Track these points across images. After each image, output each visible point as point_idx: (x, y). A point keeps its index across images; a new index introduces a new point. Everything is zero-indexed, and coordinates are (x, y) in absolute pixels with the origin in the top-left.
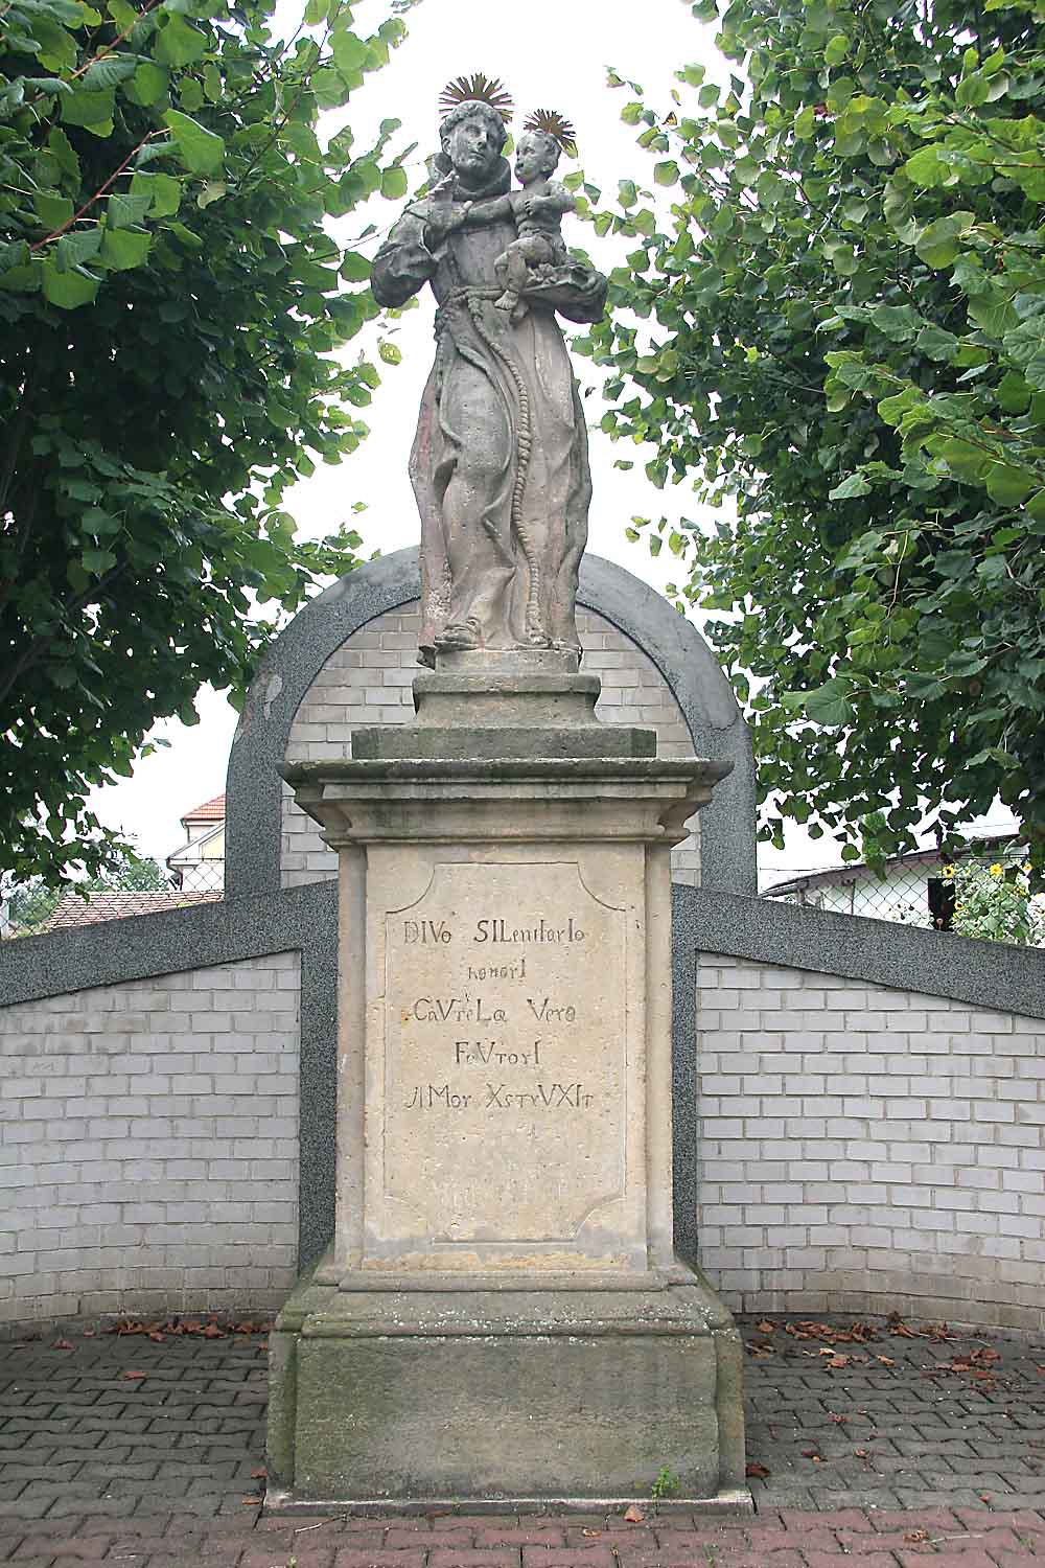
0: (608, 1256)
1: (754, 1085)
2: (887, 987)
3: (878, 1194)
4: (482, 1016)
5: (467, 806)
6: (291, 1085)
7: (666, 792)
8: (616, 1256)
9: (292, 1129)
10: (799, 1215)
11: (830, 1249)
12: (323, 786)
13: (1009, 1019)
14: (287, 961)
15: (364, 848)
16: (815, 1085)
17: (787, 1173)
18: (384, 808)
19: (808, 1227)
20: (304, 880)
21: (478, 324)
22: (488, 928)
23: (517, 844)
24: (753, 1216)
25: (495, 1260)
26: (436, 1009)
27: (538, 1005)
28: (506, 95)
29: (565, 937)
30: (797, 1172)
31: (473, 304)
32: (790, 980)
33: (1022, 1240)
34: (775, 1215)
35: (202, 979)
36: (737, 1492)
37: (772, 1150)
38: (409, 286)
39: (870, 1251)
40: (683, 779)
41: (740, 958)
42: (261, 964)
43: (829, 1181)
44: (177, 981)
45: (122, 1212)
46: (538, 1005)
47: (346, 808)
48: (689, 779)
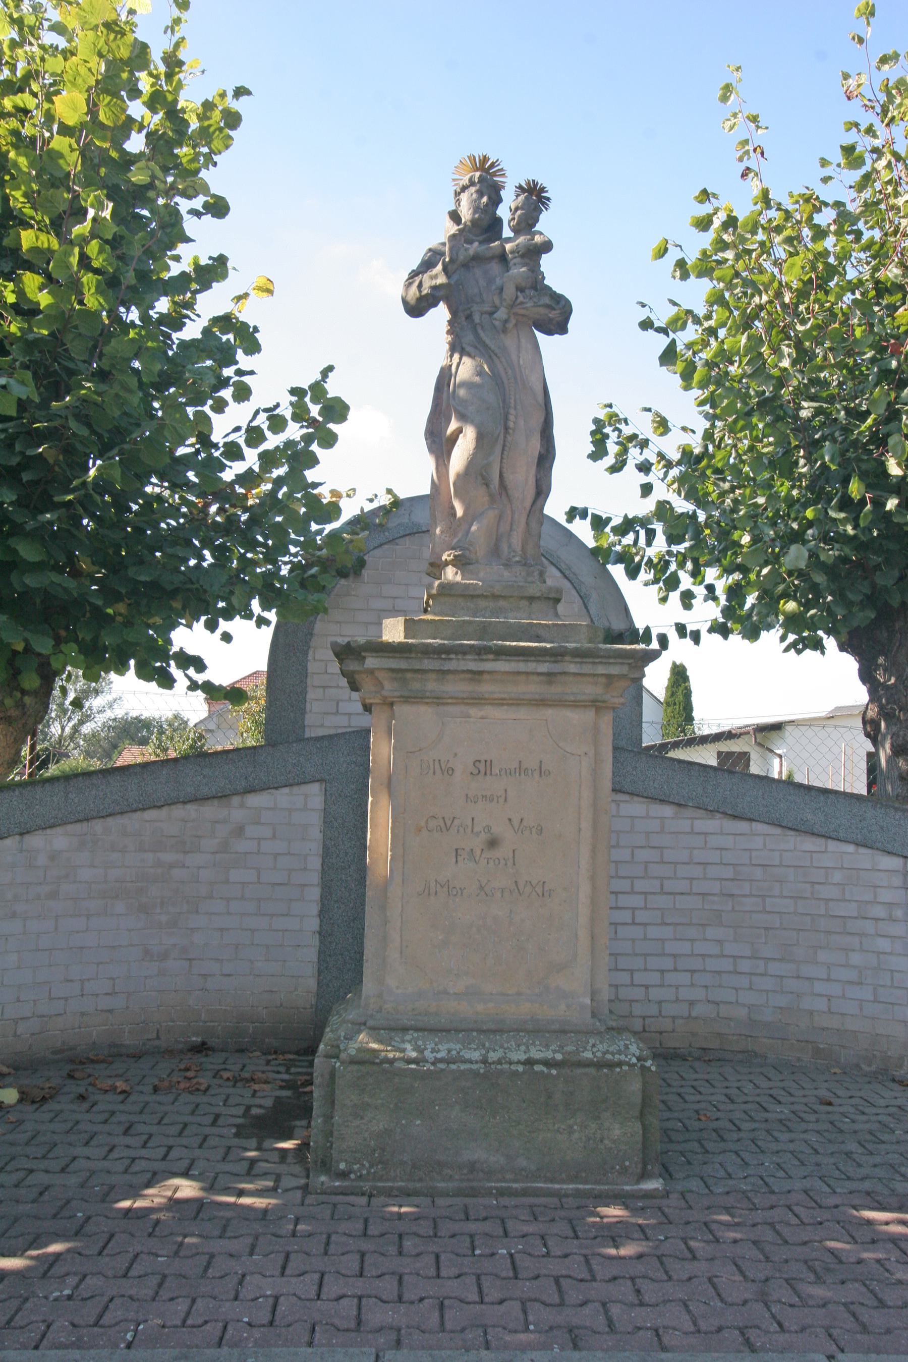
0: (563, 1007)
1: (640, 885)
2: (735, 817)
3: (726, 965)
4: (476, 830)
5: (469, 676)
6: (315, 878)
7: (615, 670)
8: (568, 1006)
9: (315, 909)
10: (671, 978)
11: (692, 1003)
12: (364, 658)
13: (823, 840)
14: (315, 788)
15: (392, 704)
16: (683, 886)
17: (663, 948)
18: (409, 675)
19: (677, 987)
20: (321, 732)
21: (482, 334)
22: (482, 766)
23: (503, 705)
24: (639, 978)
25: (480, 1007)
26: (442, 825)
27: (516, 823)
28: (502, 170)
29: (536, 774)
30: (670, 948)
31: (477, 318)
32: (668, 811)
33: (829, 998)
34: (654, 978)
35: (254, 800)
36: (654, 1181)
37: (653, 932)
38: (431, 301)
39: (721, 1006)
40: (626, 661)
41: (632, 794)
42: (296, 789)
43: (692, 955)
44: (236, 800)
45: (190, 966)
46: (516, 823)
47: (381, 675)
48: (630, 661)
